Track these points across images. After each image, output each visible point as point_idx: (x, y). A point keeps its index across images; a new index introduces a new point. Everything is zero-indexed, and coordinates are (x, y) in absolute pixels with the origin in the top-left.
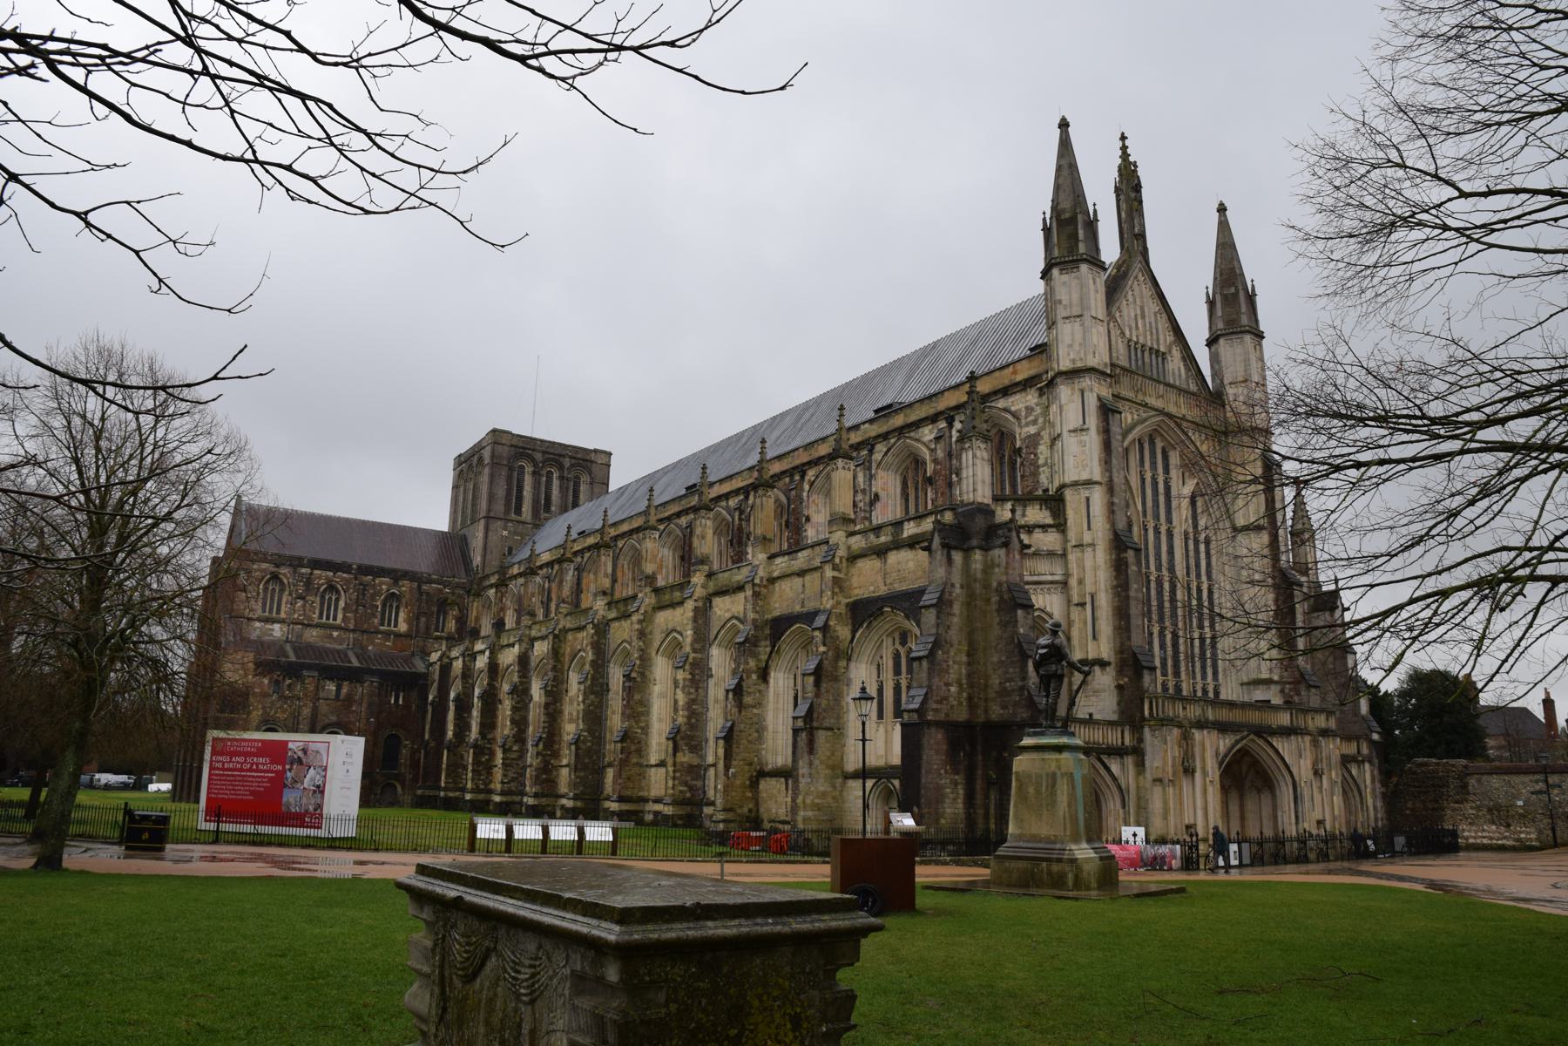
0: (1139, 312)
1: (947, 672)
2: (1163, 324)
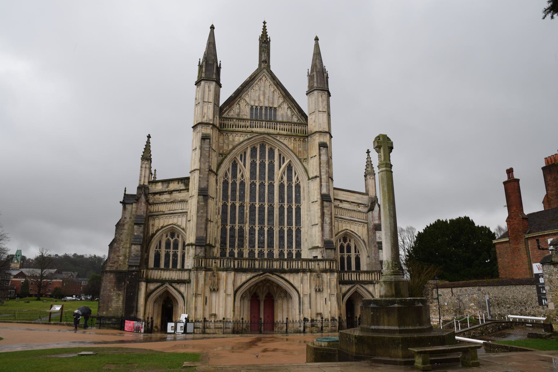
0: (261, 92)
1: (119, 251)
2: (277, 94)
